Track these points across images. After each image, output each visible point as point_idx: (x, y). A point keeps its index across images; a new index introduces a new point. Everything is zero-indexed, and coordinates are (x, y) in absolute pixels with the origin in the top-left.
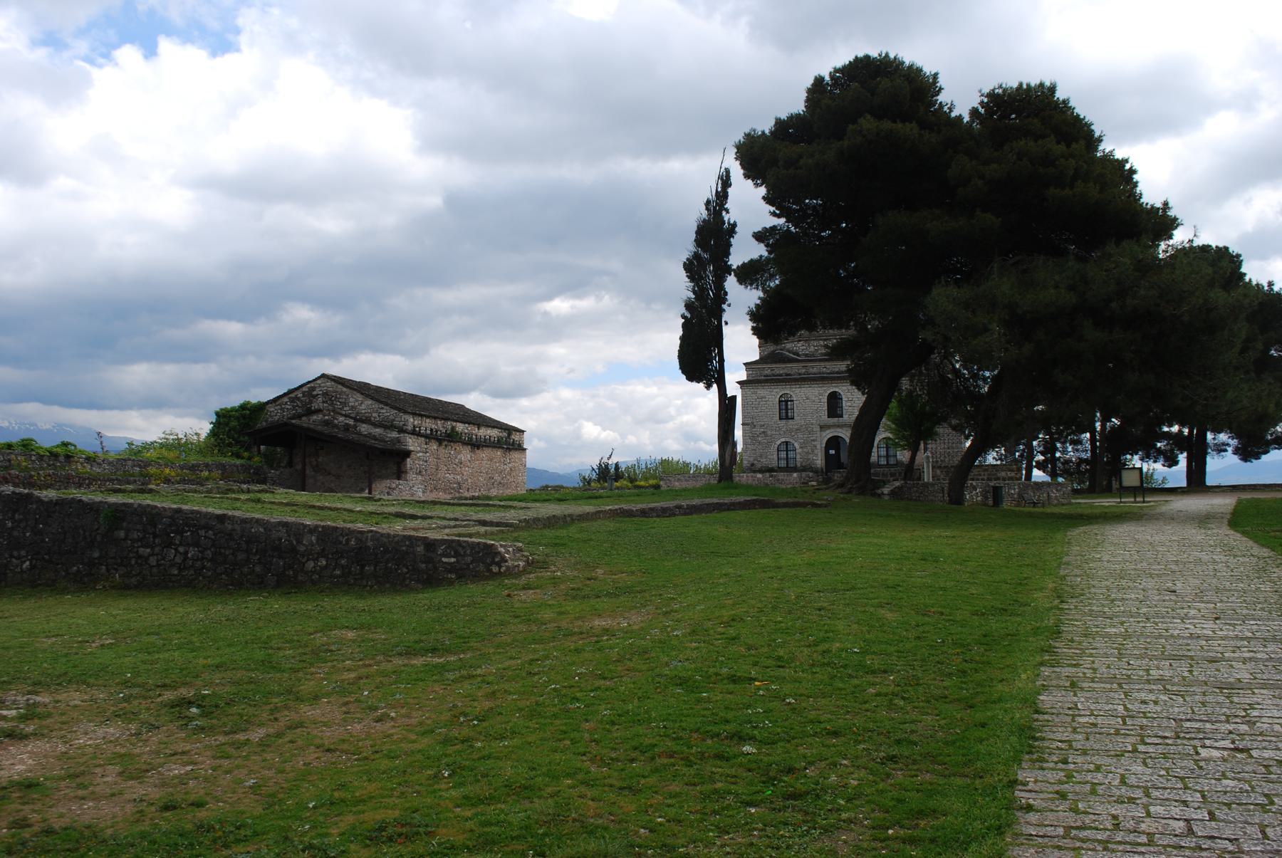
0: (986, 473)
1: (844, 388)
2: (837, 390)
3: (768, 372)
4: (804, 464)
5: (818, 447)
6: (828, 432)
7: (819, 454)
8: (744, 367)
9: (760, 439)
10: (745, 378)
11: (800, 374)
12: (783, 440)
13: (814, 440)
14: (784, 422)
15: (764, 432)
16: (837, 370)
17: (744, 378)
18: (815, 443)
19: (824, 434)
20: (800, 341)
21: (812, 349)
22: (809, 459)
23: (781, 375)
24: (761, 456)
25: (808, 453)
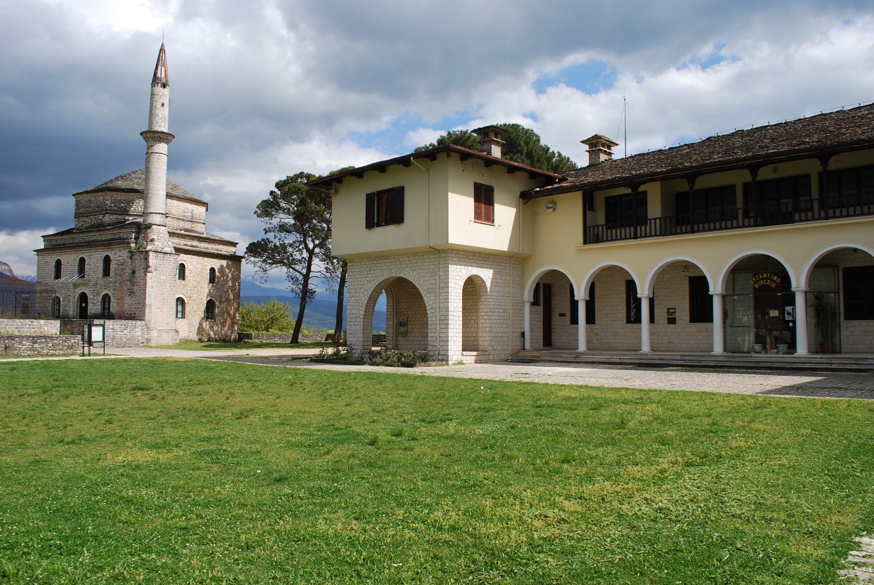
1: (87, 254)
2: (83, 256)
3: (54, 243)
6: (79, 289)
7: (72, 306)
10: (42, 247)
11: (70, 244)
13: (69, 296)
16: (88, 240)
19: (77, 290)
22: (66, 310)
23: (60, 245)
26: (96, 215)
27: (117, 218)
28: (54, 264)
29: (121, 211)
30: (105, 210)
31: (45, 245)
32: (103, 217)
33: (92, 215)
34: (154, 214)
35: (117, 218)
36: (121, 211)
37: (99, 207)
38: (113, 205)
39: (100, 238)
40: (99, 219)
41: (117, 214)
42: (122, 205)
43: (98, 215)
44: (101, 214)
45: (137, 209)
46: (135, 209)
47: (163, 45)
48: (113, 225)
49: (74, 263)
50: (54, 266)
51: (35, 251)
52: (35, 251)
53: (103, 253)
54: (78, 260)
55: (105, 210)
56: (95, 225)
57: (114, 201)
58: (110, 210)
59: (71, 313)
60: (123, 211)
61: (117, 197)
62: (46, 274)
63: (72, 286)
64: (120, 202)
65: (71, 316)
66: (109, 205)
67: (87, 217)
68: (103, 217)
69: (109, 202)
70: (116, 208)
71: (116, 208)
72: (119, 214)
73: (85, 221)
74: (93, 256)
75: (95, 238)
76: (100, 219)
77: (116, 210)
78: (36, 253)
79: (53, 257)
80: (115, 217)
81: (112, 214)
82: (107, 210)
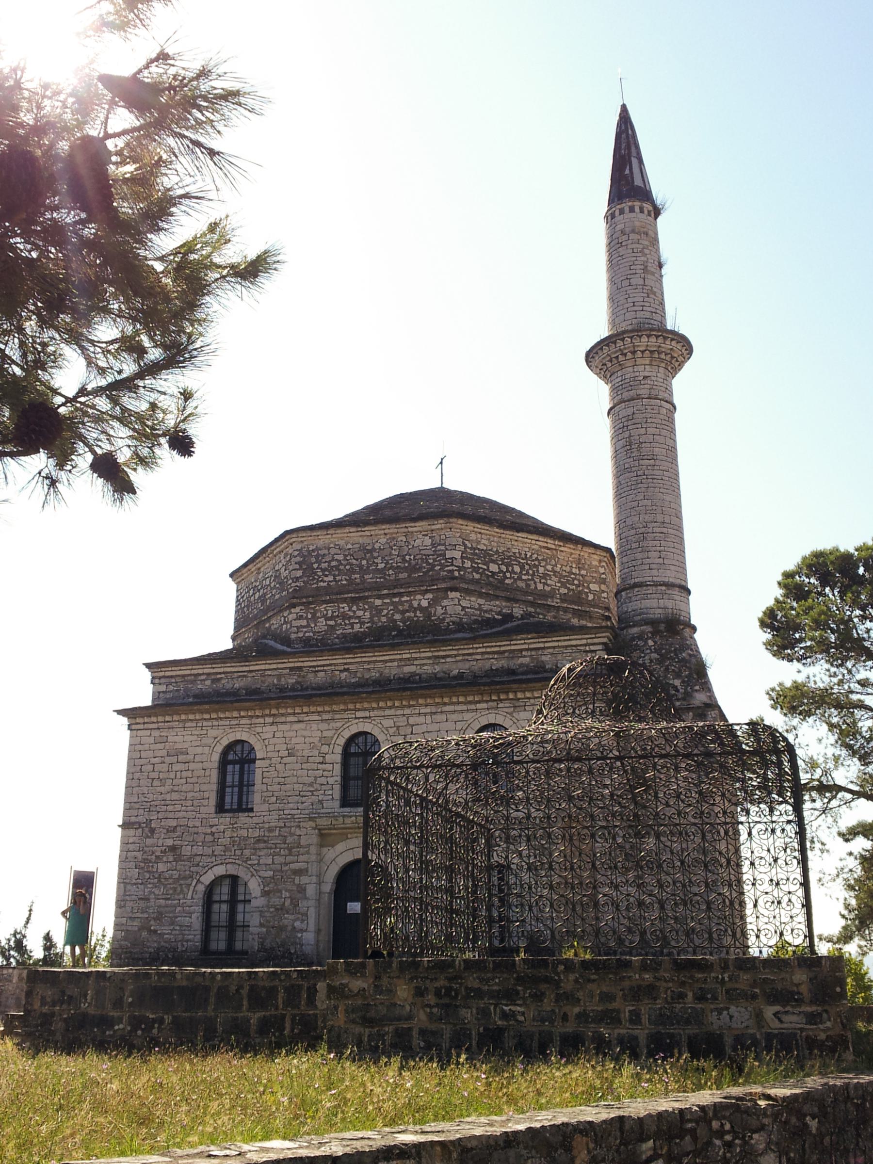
0: (645, 1009)
1: (388, 723)
2: (367, 727)
4: (268, 944)
5: (311, 891)
6: (340, 847)
7: (312, 912)
8: (147, 675)
9: (161, 867)
10: (147, 701)
12: (220, 870)
13: (299, 872)
14: (226, 819)
15: (173, 848)
16: (374, 674)
17: (143, 696)
18: (305, 880)
19: (330, 853)
20: (294, 606)
21: (322, 625)
22: (282, 929)
24: (159, 917)
25: (281, 909)
26: (401, 595)
27: (480, 609)
28: (216, 757)
29: (490, 584)
30: (444, 579)
31: (156, 696)
32: (434, 602)
33: (379, 597)
34: (676, 591)
35: (480, 609)
36: (490, 584)
37: (413, 569)
38: (468, 564)
39: (438, 668)
40: (412, 609)
41: (481, 595)
42: (494, 568)
43: (409, 594)
44: (426, 591)
45: (533, 587)
46: (528, 586)
47: (624, 108)
48: (472, 630)
49: (323, 755)
50: (216, 765)
51: (122, 712)
52: (122, 712)
53: (467, 716)
54: (342, 741)
55: (444, 579)
56: (396, 628)
57: (474, 553)
58: (462, 578)
59: (309, 937)
60: (497, 588)
61: (478, 543)
62: (175, 796)
63: (309, 838)
64: (487, 556)
65: (308, 949)
66: (458, 563)
67: (354, 600)
68: (434, 602)
69: (457, 554)
70: (477, 576)
71: (477, 576)
72: (487, 596)
73: (344, 616)
74: (416, 729)
75: (408, 669)
76: (421, 609)
77: (477, 582)
78: (125, 721)
79: (213, 733)
80: (473, 602)
81: (468, 592)
82: (456, 578)
